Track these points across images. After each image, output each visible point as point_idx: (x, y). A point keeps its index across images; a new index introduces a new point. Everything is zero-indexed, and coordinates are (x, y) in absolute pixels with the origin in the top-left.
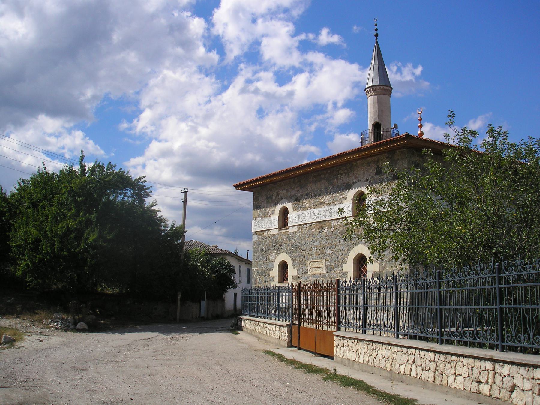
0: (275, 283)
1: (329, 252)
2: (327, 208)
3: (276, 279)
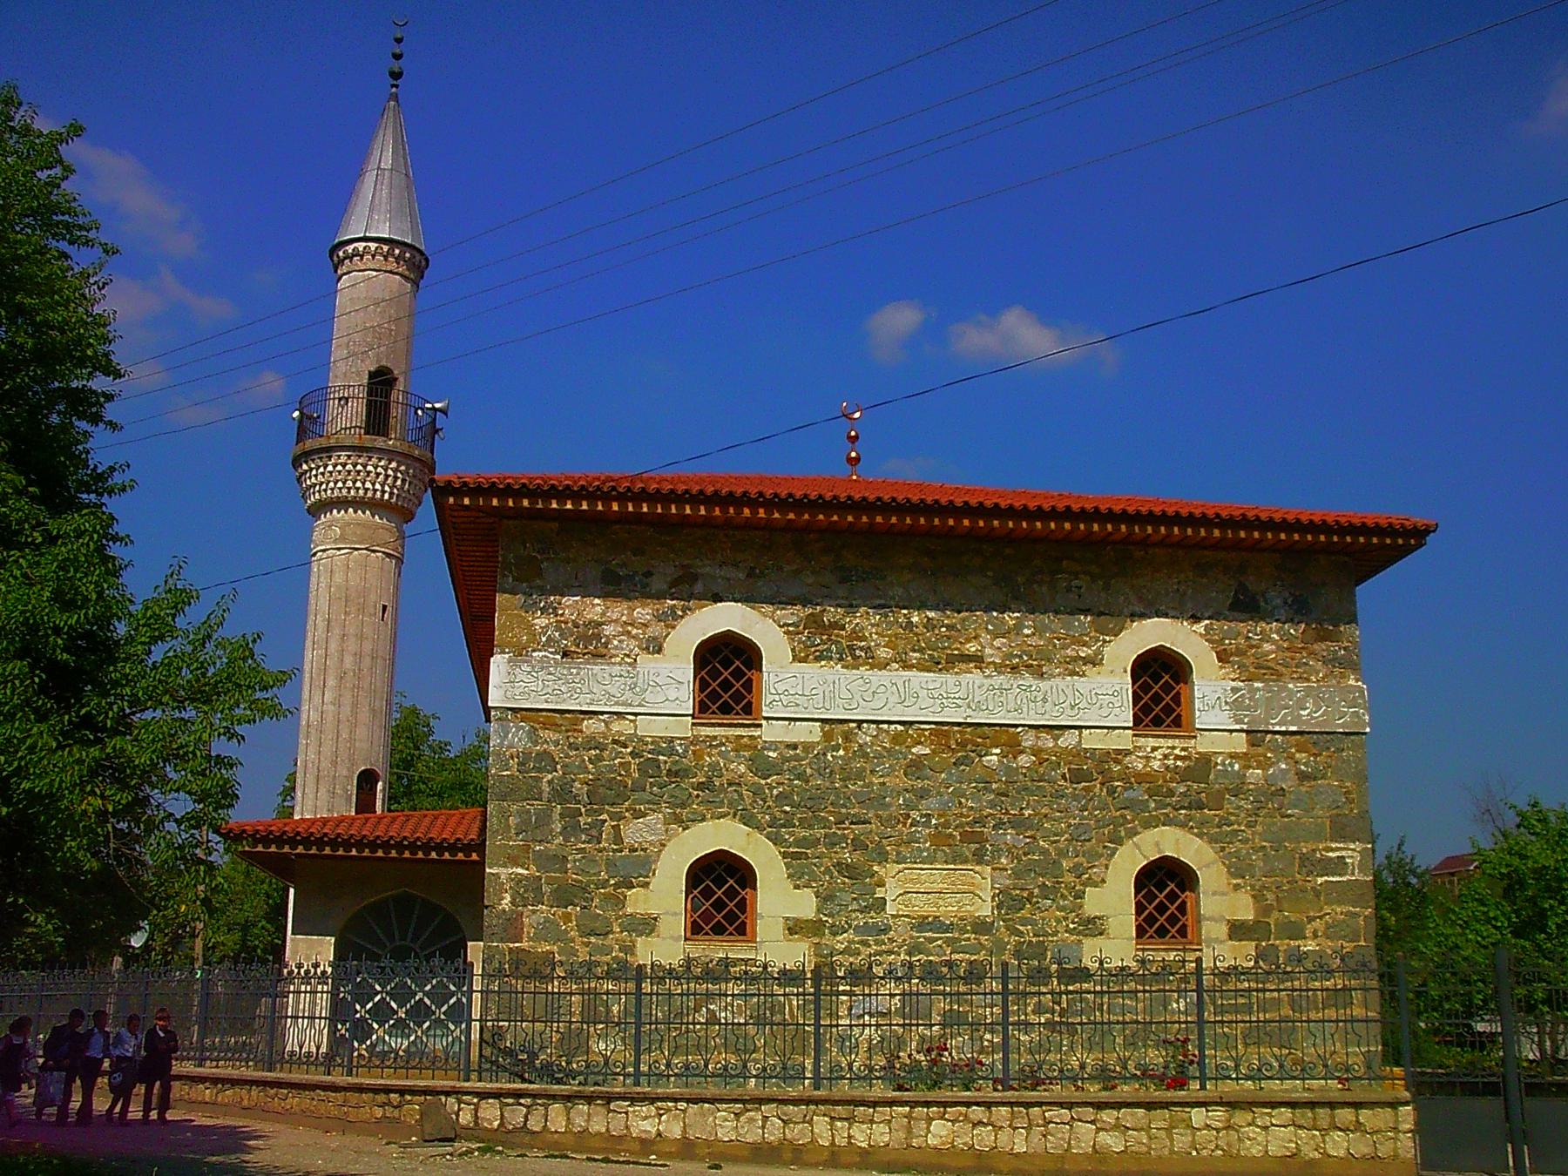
0: (667, 947)
2: (1000, 680)
3: (679, 925)
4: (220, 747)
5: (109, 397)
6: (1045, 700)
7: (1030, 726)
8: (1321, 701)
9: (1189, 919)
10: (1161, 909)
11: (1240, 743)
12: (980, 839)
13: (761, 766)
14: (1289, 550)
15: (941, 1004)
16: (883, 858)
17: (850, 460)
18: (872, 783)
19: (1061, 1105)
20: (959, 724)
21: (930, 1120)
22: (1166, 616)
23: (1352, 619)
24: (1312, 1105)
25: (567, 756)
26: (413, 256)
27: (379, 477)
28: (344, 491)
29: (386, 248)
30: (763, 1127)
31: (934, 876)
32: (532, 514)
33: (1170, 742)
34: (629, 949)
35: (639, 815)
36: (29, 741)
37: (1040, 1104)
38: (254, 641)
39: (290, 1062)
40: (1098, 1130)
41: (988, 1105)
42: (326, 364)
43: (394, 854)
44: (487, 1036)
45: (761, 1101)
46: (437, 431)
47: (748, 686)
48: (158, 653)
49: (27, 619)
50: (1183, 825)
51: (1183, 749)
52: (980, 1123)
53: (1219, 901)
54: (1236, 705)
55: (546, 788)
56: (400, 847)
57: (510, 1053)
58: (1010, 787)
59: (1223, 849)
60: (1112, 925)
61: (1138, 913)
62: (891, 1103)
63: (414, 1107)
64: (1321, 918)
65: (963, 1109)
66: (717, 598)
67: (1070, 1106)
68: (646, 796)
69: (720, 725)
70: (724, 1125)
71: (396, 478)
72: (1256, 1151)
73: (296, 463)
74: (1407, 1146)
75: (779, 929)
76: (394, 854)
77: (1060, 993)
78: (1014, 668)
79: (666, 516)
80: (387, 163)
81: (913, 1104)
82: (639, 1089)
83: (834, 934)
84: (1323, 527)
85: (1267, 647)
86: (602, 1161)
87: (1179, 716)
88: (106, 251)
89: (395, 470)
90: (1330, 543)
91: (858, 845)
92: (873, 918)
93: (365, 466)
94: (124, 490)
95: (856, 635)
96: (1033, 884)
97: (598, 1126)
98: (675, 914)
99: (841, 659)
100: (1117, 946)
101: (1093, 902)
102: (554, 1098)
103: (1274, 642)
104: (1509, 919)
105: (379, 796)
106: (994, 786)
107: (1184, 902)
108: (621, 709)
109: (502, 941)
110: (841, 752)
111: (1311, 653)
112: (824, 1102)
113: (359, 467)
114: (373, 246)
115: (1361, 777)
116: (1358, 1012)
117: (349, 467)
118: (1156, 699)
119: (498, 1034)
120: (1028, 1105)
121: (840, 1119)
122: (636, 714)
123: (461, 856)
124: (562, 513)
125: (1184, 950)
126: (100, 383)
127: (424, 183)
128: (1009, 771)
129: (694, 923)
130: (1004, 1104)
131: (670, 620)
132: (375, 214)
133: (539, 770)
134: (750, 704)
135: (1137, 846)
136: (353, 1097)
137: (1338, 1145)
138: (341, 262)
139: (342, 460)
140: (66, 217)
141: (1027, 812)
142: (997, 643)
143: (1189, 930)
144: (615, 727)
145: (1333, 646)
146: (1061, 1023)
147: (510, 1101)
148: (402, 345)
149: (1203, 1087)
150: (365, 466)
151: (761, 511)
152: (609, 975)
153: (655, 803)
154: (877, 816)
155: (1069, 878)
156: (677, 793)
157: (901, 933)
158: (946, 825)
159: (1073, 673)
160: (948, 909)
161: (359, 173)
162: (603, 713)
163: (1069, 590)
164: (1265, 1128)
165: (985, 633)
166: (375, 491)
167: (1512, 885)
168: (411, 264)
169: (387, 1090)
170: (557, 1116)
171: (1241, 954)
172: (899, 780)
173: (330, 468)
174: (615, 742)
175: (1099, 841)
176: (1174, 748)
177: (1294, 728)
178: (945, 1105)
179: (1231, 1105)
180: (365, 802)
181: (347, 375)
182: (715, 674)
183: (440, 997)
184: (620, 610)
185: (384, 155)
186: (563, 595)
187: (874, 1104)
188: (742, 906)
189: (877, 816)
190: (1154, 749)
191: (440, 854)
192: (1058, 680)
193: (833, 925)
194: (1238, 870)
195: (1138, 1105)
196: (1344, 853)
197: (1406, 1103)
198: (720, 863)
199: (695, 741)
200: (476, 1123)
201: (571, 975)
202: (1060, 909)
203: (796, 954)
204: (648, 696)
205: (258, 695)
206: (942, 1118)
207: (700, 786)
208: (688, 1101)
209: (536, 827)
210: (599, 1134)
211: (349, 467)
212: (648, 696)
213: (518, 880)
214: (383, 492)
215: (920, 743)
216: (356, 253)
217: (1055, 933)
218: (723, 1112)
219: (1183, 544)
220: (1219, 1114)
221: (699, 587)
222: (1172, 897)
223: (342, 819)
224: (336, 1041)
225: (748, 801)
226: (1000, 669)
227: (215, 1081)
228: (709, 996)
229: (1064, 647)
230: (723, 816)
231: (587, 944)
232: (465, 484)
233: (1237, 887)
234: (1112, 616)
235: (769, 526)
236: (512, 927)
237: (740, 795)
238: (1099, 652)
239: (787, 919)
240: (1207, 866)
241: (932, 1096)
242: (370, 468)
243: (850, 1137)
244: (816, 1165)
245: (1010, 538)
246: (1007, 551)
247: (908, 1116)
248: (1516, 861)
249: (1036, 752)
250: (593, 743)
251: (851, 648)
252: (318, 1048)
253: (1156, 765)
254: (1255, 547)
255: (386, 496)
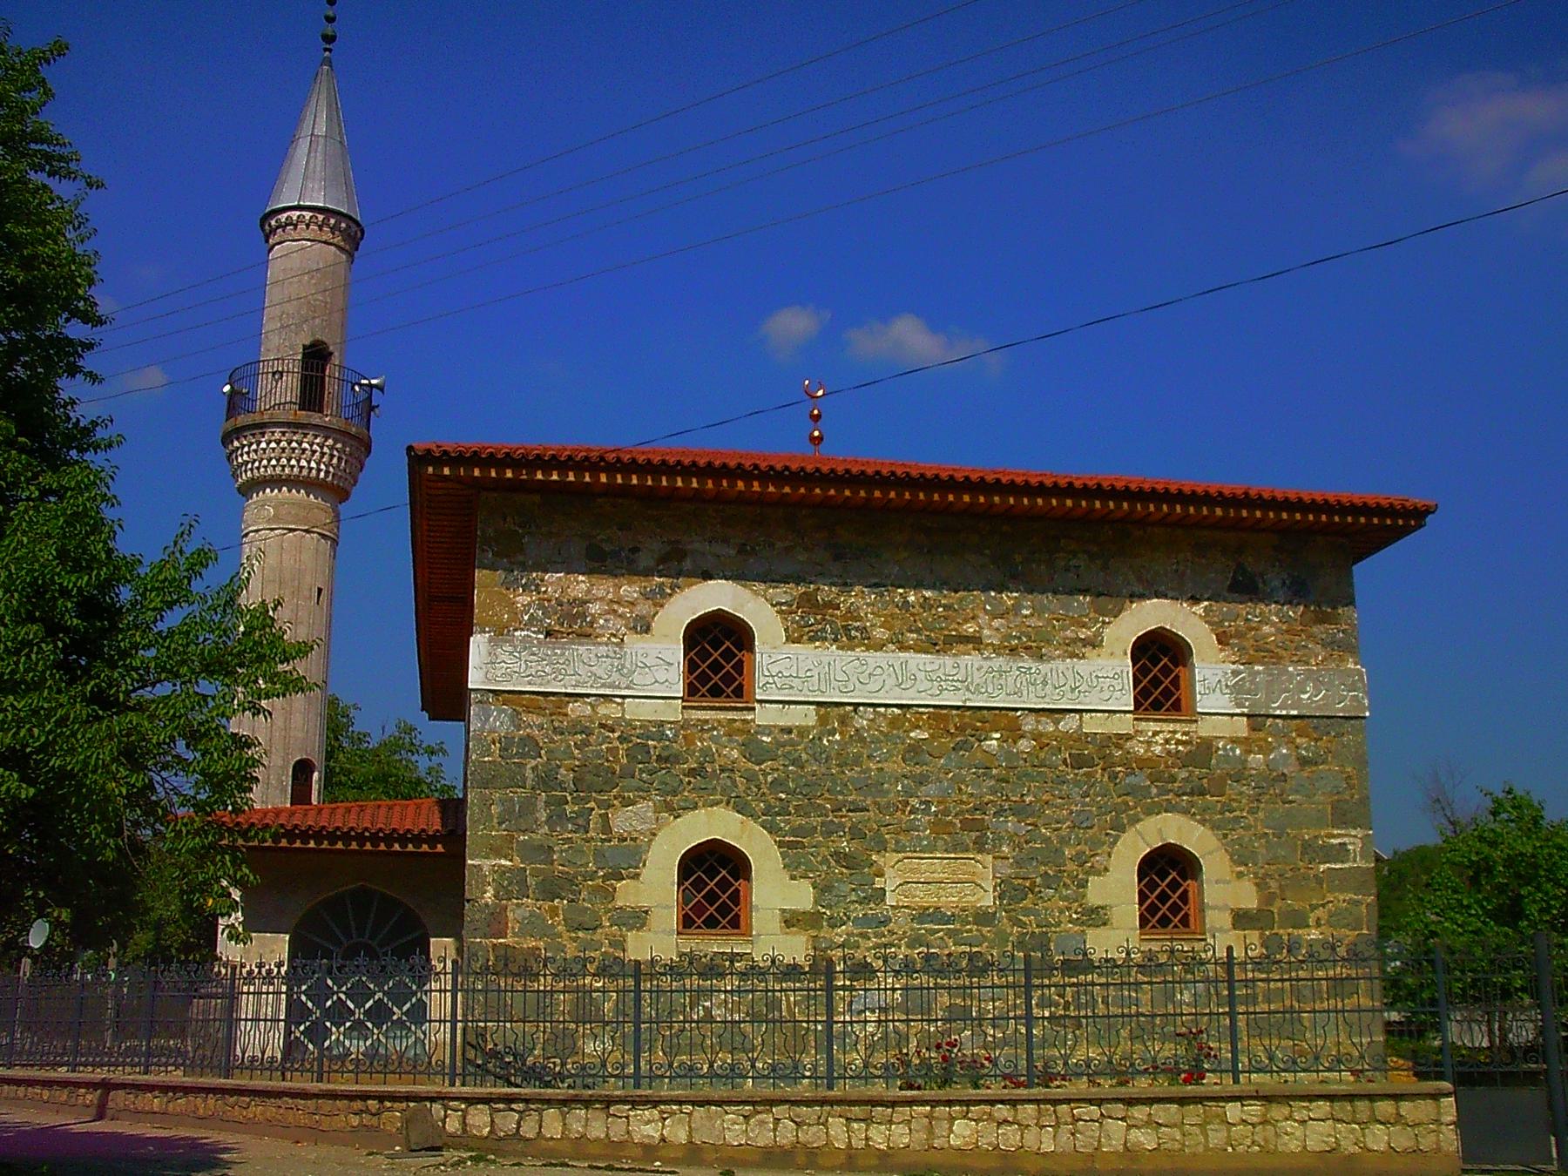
0: (659, 940)
1: (1011, 823)
2: (999, 662)
3: (673, 919)
4: (241, 725)
5: (89, 346)
6: (1045, 683)
7: (1031, 710)
8: (1321, 684)
9: (1191, 908)
10: (1163, 897)
11: (1241, 727)
12: (981, 827)
13: (753, 750)
14: (1280, 529)
15: (945, 999)
16: (882, 847)
17: (813, 439)
18: (870, 770)
19: (1090, 1102)
20: (958, 708)
21: (952, 1119)
22: (1166, 597)
23: (1350, 601)
24: (1351, 1097)
25: (552, 741)
26: (348, 227)
27: (314, 455)
28: (278, 469)
29: (321, 217)
30: (775, 1130)
31: (934, 866)
32: (515, 486)
33: (1171, 727)
34: (620, 944)
35: (627, 803)
36: (60, 712)
37: (1068, 1101)
38: (274, 609)
39: (242, 1067)
40: (1129, 1127)
41: (1013, 1103)
42: (258, 335)
43: (354, 846)
44: (471, 1038)
45: (772, 1102)
46: (372, 408)
47: (739, 667)
48: (173, 619)
49: (36, 579)
50: (1185, 812)
51: (1184, 734)
52: (1006, 1121)
53: (1223, 889)
54: (1237, 689)
55: (529, 774)
56: (361, 839)
57: (494, 1054)
58: (1010, 773)
59: (1225, 836)
60: (1116, 915)
61: (1141, 903)
62: (911, 1103)
63: (394, 1116)
64: (1323, 906)
65: (987, 1108)
66: (707, 576)
67: (1099, 1102)
68: (635, 782)
69: (712, 708)
70: (732, 1128)
71: (332, 456)
72: (1294, 1146)
73: (227, 439)
74: (1450, 1139)
75: (776, 924)
76: (354, 846)
77: (1064, 986)
78: (1013, 650)
79: (657, 487)
80: (321, 129)
81: (934, 1103)
82: (639, 1092)
83: (833, 926)
84: (1326, 507)
85: (1266, 629)
86: (606, 1168)
87: (1178, 700)
88: (90, 185)
89: (332, 448)
90: (1331, 523)
91: (856, 833)
92: (872, 910)
93: (300, 444)
94: (110, 446)
95: (852, 614)
96: (1036, 872)
97: (597, 1130)
98: (667, 907)
99: (835, 640)
100: (1120, 934)
101: (1096, 892)
102: (549, 1102)
103: (1273, 624)
104: (1483, 907)
105: (315, 786)
106: (994, 771)
107: (1186, 891)
108: (608, 692)
109: (485, 937)
110: (837, 737)
111: (1310, 636)
112: (840, 1102)
113: (294, 445)
114: (308, 215)
115: (1361, 761)
116: (1365, 1002)
117: (283, 444)
118: (1156, 682)
119: (481, 1035)
120: (1056, 1102)
121: (858, 1120)
122: (623, 697)
123: (425, 847)
124: (545, 486)
125: (1171, 940)
126: (76, 330)
127: (358, 150)
128: (1009, 756)
129: (686, 916)
130: (1030, 1101)
131: (658, 598)
132: (308, 180)
133: (523, 756)
134: (741, 686)
135: (1139, 832)
136: (327, 1105)
137: (1378, 1139)
138: (273, 231)
139: (277, 436)
140: (45, 147)
141: (1028, 799)
142: (996, 623)
143: (1192, 919)
144: (602, 710)
145: (1332, 629)
146: (1065, 1017)
147: (501, 1106)
148: (337, 317)
149: (1236, 1081)
150: (300, 444)
151: (756, 484)
152: (601, 972)
153: (644, 791)
154: (875, 803)
155: (1071, 866)
156: (668, 780)
157: (901, 924)
158: (946, 812)
159: (1073, 655)
160: (949, 899)
161: (293, 140)
162: (588, 696)
163: (1067, 570)
164: (1303, 1122)
165: (984, 612)
166: (311, 469)
167: (1478, 872)
168: (346, 235)
169: (365, 1097)
170: (553, 1123)
171: (1246, 944)
172: (896, 766)
173: (263, 445)
174: (602, 726)
175: (1101, 829)
176: (1175, 732)
177: (1295, 713)
178: (968, 1103)
179: (1268, 1099)
180: (300, 794)
181: (280, 346)
182: (704, 655)
183: (399, 997)
184: (604, 588)
185: (318, 121)
186: (546, 571)
187: (893, 1104)
188: (735, 897)
189: (875, 803)
190: (1155, 734)
191: (404, 846)
192: (1059, 661)
193: (831, 918)
194: (1241, 857)
195: (1170, 1100)
196: (1346, 840)
197: (1448, 1095)
198: (712, 853)
199: (685, 725)
200: (464, 1131)
201: (564, 972)
202: (1062, 899)
203: (795, 949)
204: (636, 678)
205: (280, 667)
206: (964, 1117)
207: (692, 772)
208: (693, 1103)
209: (518, 816)
210: (597, 1140)
211: (283, 444)
212: (636, 678)
213: (502, 871)
214: (319, 470)
215: (918, 727)
216: (289, 222)
217: (1058, 924)
218: (731, 1116)
219: (1183, 523)
220: (1254, 1109)
221: (687, 564)
222: (1174, 885)
223: (278, 812)
224: (290, 1046)
225: (742, 788)
226: (997, 650)
227: (165, 1089)
228: (701, 992)
229: (1063, 629)
230: (717, 803)
231: (575, 940)
232: (445, 452)
233: (1240, 875)
234: (1112, 594)
235: (761, 500)
236: (496, 922)
237: (734, 782)
238: (1099, 634)
239: (783, 911)
240: (1210, 853)
241: (942, 1094)
242: (305, 445)
243: (867, 1139)
244: (832, 1169)
245: (1009, 515)
246: (1005, 528)
247: (929, 1116)
248: (1486, 850)
249: (1037, 736)
250: (579, 727)
251: (846, 628)
252: (263, 1053)
253: (1158, 749)
254: (1256, 527)
255: (322, 475)
